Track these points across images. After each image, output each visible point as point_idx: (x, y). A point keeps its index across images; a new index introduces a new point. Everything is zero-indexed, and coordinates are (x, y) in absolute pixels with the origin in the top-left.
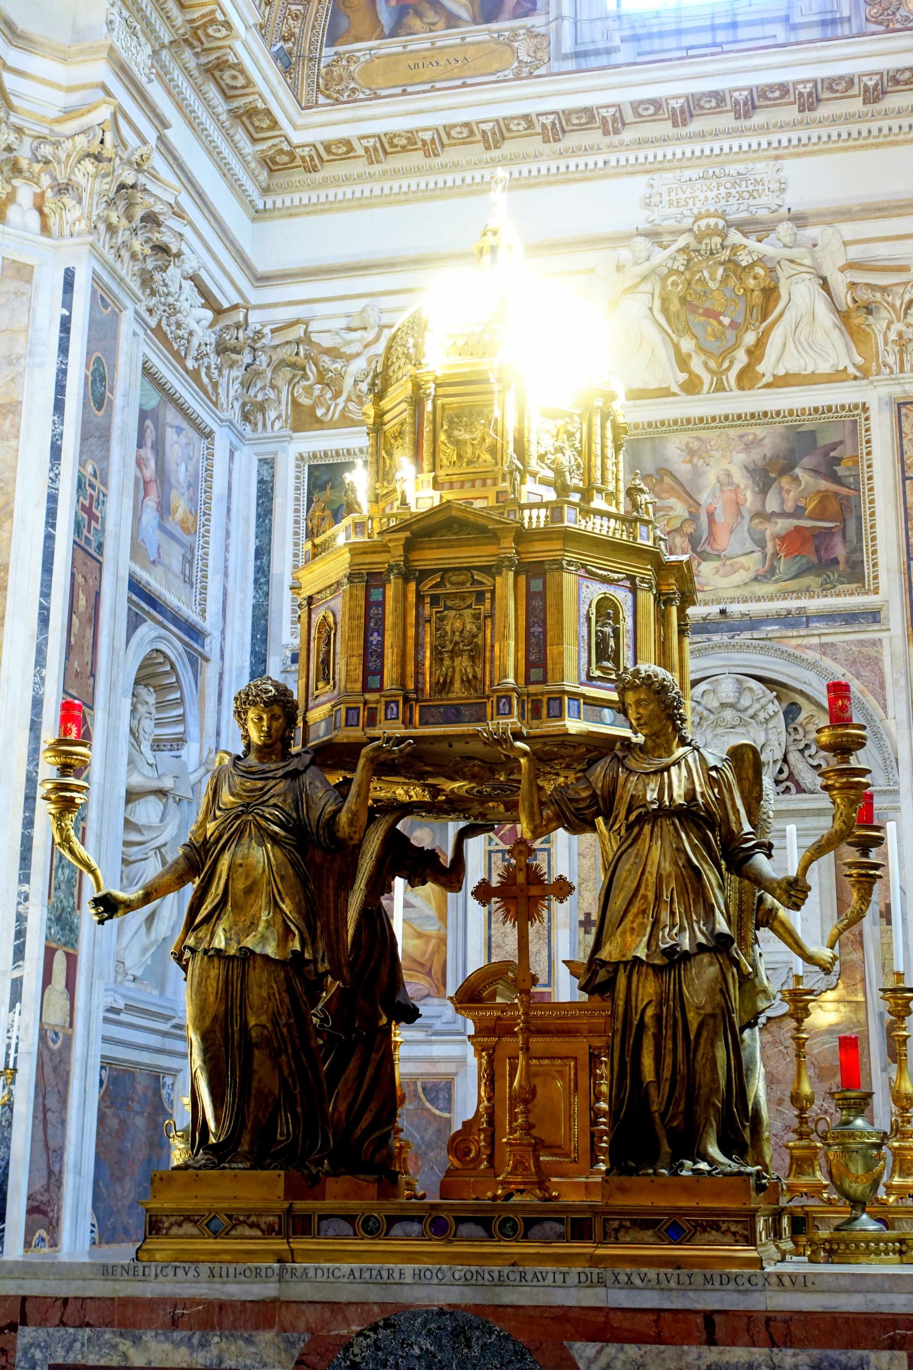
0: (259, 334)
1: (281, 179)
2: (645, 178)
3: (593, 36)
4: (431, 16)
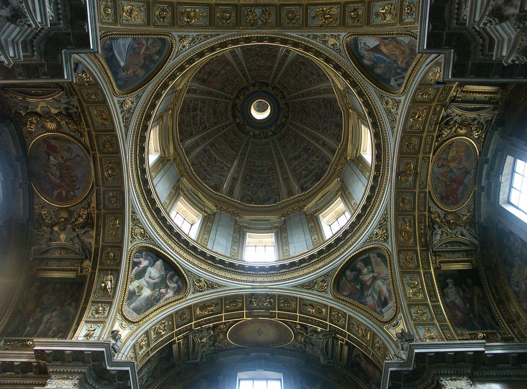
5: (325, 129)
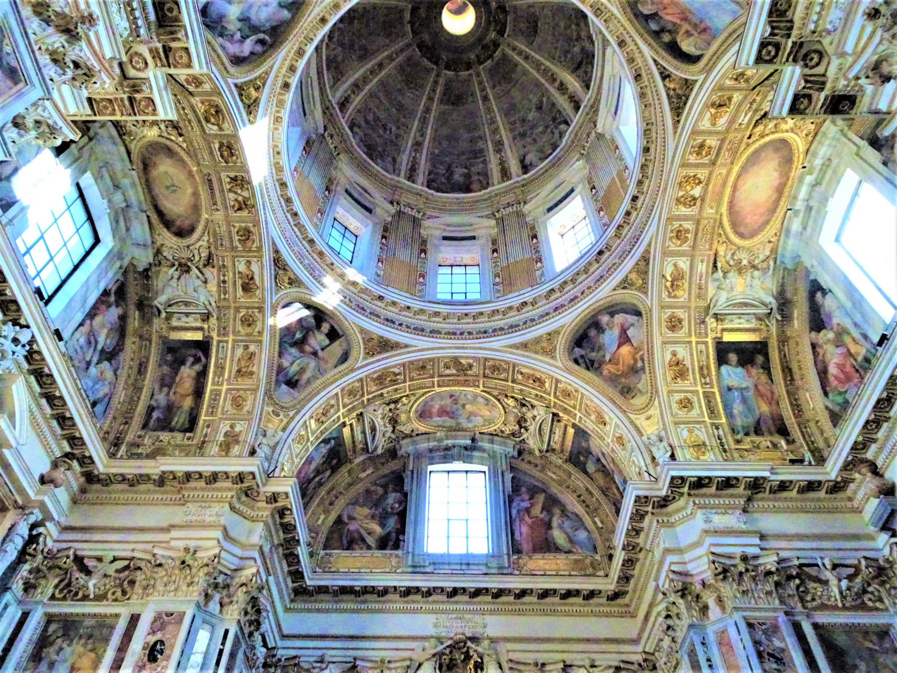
0: (280, 660)
1: (300, 598)
2: (435, 616)
5: (440, 144)
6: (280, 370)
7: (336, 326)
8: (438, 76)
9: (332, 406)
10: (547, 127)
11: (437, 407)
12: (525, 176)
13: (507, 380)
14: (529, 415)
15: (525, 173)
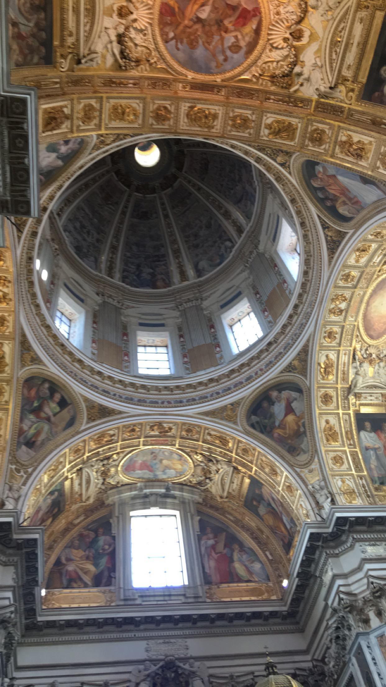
3: (129, 594)
4: (80, 583)
6: (21, 432)
7: (66, 397)
8: (130, 196)
9: (61, 462)
10: (215, 242)
11: (140, 462)
12: (201, 279)
13: (198, 441)
14: (213, 468)
15: (199, 276)
